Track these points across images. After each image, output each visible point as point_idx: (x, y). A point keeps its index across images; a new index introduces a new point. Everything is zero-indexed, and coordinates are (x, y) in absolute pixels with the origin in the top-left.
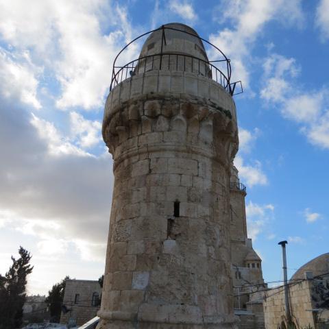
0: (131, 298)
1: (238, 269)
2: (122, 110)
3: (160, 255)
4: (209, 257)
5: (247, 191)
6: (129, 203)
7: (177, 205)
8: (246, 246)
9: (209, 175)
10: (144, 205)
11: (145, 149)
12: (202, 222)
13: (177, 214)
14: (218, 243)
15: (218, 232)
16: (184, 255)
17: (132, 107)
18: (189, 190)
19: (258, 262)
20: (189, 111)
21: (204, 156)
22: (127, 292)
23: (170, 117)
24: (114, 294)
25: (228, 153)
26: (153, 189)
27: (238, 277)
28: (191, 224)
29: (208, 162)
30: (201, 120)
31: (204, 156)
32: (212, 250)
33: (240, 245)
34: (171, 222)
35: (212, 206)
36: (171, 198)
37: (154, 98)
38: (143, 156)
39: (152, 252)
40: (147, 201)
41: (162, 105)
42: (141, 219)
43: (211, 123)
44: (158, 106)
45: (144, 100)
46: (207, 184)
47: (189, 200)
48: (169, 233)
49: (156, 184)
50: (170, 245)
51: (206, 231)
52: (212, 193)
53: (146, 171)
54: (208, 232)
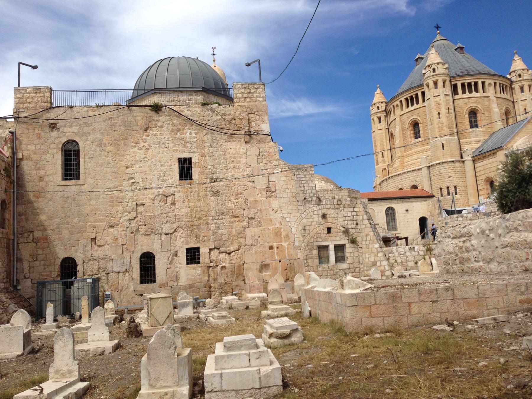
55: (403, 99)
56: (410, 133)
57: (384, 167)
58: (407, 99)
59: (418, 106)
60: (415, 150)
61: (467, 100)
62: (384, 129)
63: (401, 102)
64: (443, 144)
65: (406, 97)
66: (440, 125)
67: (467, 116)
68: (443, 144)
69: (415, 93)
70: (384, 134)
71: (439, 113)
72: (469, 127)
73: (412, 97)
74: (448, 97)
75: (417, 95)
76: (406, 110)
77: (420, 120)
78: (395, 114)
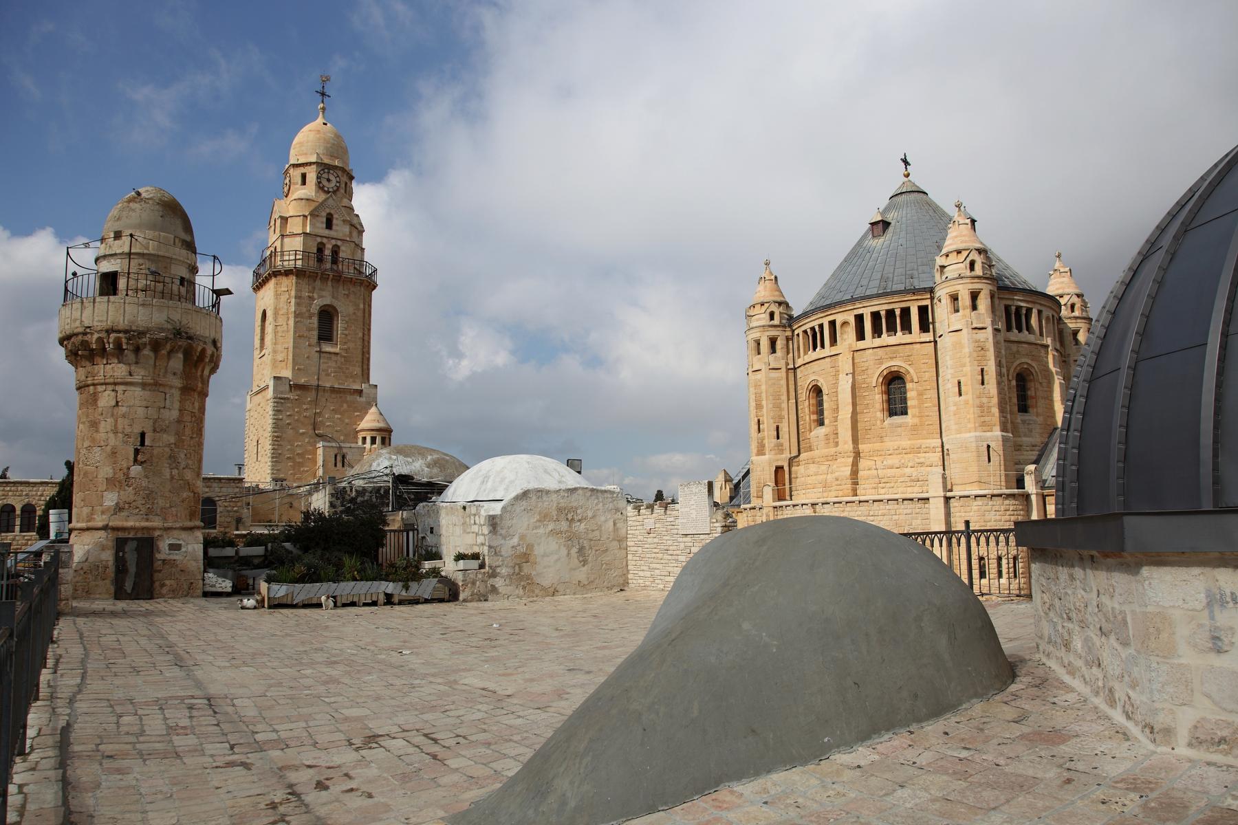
0: (103, 513)
1: (340, 448)
2: (85, 334)
3: (127, 477)
4: (172, 477)
5: (379, 279)
6: (97, 431)
7: (143, 435)
8: (363, 399)
9: (177, 405)
10: (111, 435)
11: (111, 380)
12: (167, 449)
13: (142, 443)
14: (183, 464)
15: (183, 456)
16: (146, 477)
17: (96, 336)
18: (155, 421)
19: (384, 434)
20: (156, 346)
21: (171, 387)
22: (99, 508)
23: (137, 350)
24: (86, 510)
25: (202, 376)
26: (120, 420)
27: (339, 464)
28: (155, 452)
29: (177, 394)
30: (170, 352)
31: (171, 387)
32: (175, 472)
33: (349, 398)
34: (137, 452)
35: (177, 434)
36: (137, 430)
37: (119, 332)
38: (111, 387)
39: (120, 476)
40: (115, 432)
41: (129, 339)
42: (109, 448)
43: (181, 355)
44: (124, 341)
45: (109, 331)
46: (175, 414)
47: (154, 431)
48: (135, 460)
49: (124, 416)
50: (136, 470)
51: (170, 457)
52: (179, 421)
53: (114, 403)
54: (172, 457)
55: (867, 314)
56: (876, 399)
57: (780, 464)
58: (876, 316)
59: (907, 338)
60: (895, 444)
61: (1014, 347)
62: (784, 370)
63: (859, 319)
64: (989, 447)
65: (875, 309)
66: (985, 400)
67: (1014, 383)
68: (989, 447)
69: (904, 305)
70: (784, 382)
71: (982, 370)
72: (1016, 408)
73: (890, 313)
74: (981, 335)
75: (906, 312)
76: (870, 340)
77: (911, 372)
78: (834, 341)
